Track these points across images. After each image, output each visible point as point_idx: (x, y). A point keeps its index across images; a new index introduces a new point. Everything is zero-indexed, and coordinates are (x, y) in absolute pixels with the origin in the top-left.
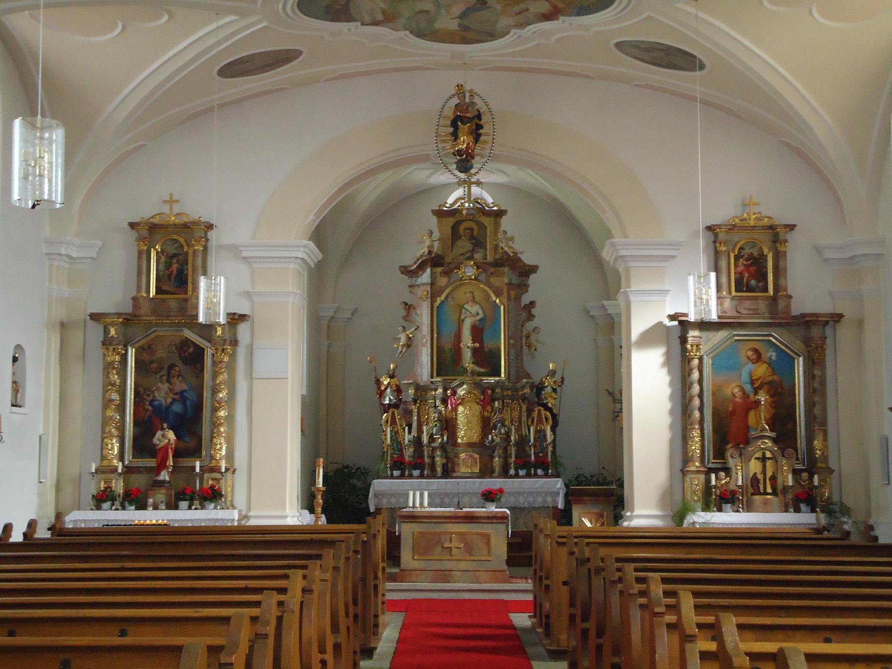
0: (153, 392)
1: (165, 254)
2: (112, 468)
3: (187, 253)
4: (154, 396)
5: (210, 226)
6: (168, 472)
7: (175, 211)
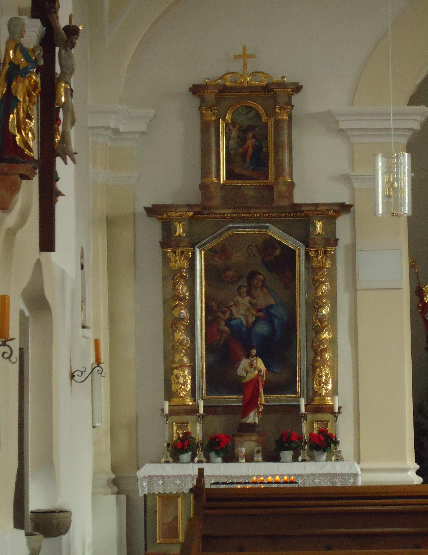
0: (229, 308)
1: (237, 126)
2: (185, 408)
3: (266, 124)
4: (231, 313)
5: (297, 88)
6: (258, 413)
7: (250, 69)
